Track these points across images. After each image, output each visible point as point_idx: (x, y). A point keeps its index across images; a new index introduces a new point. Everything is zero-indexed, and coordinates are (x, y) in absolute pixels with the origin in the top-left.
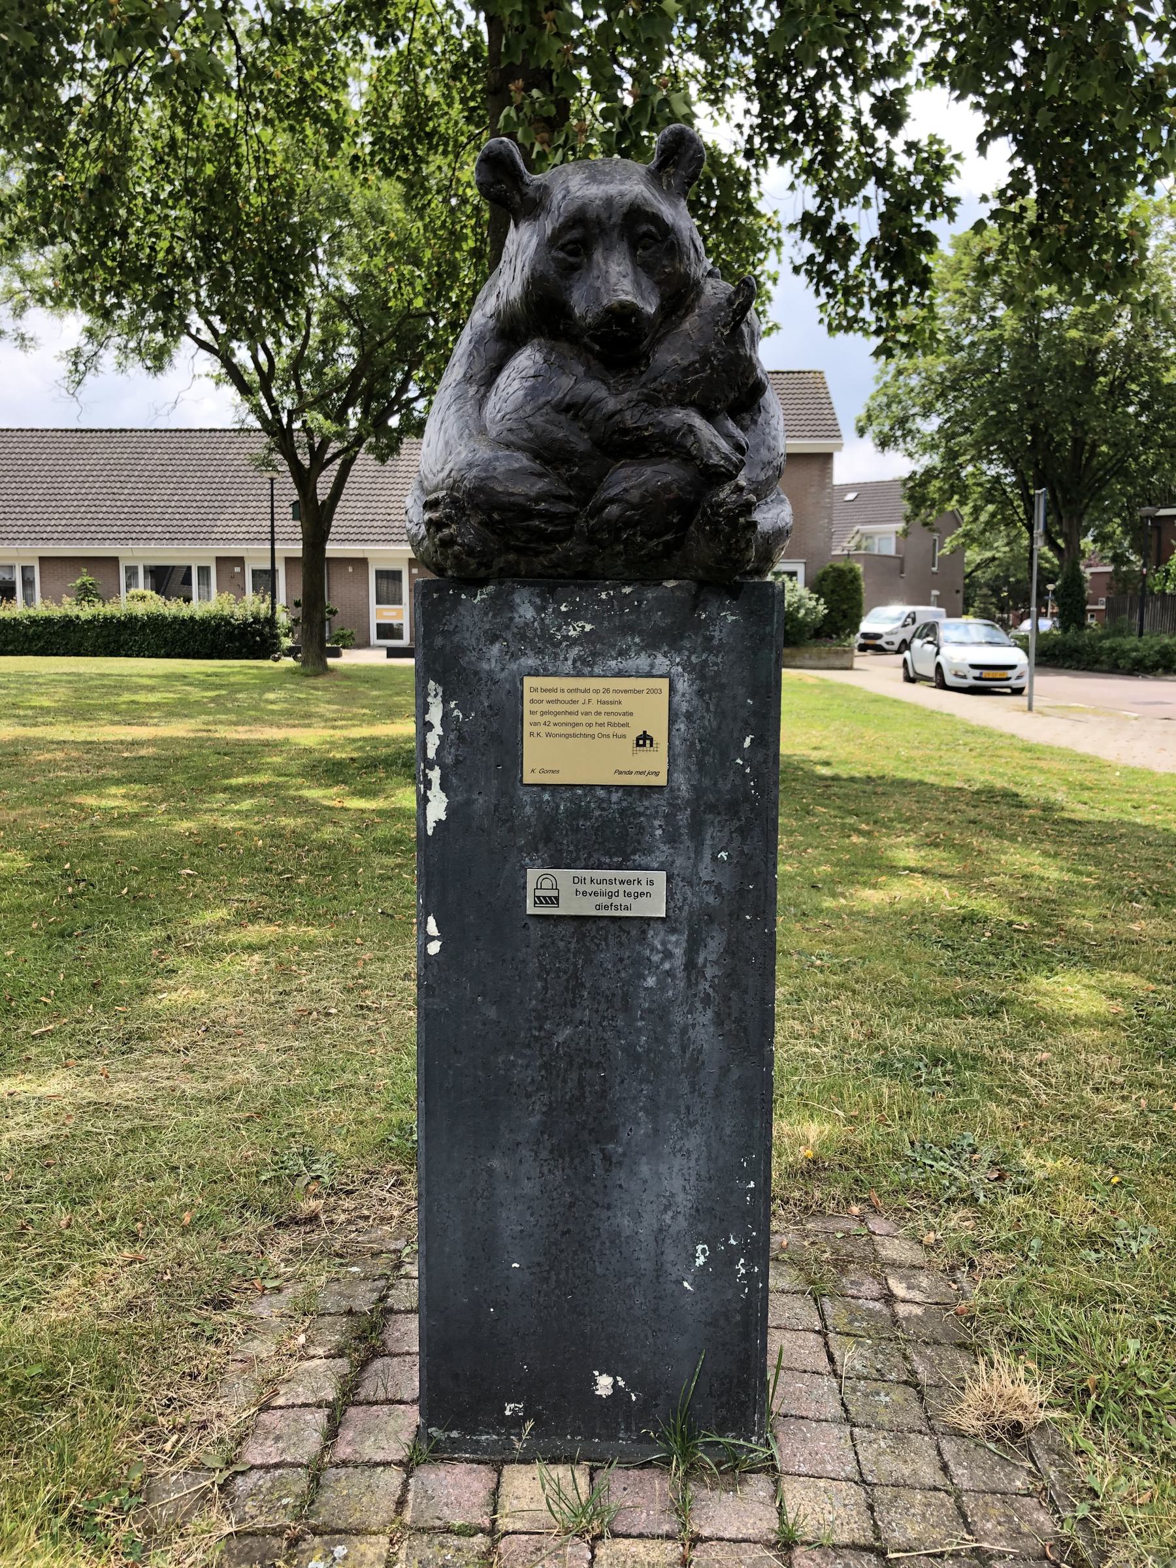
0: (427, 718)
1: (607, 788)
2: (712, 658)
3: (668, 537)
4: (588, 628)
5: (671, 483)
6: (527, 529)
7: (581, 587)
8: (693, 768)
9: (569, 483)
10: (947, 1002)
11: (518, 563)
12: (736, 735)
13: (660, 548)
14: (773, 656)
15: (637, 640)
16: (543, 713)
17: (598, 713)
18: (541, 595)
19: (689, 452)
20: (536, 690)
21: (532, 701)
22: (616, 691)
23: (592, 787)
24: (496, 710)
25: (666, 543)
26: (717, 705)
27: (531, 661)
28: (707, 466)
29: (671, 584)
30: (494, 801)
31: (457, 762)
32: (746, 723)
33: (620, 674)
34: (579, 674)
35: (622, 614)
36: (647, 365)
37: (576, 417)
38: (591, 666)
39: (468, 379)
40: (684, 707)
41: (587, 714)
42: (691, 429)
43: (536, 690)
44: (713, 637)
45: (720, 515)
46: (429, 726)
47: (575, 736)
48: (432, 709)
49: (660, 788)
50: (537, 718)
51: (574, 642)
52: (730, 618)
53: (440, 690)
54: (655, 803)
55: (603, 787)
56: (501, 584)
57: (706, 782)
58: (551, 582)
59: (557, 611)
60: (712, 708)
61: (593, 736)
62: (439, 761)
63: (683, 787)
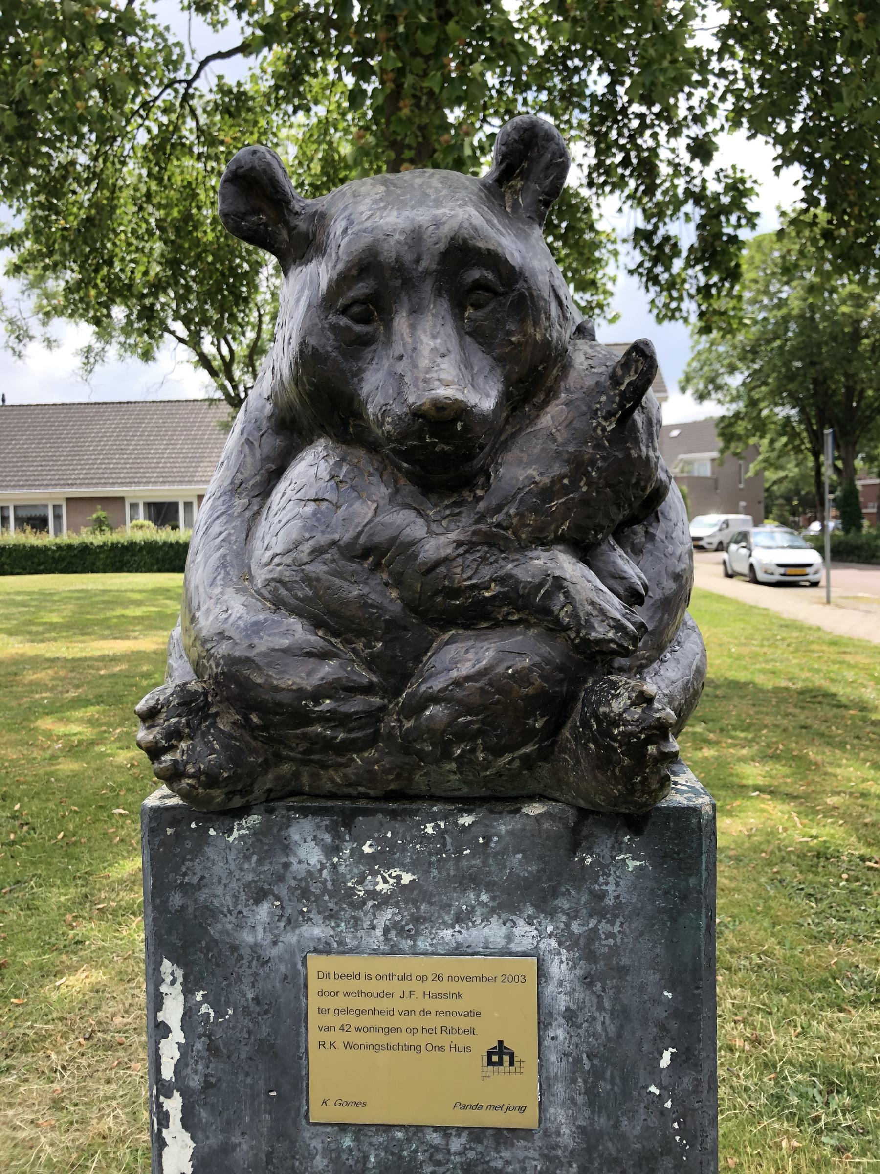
0: (161, 1016)
1: (444, 1131)
2: (604, 927)
3: (528, 749)
4: (407, 878)
5: (530, 670)
6: (305, 736)
7: (394, 815)
8: (580, 1099)
9: (371, 663)
10: (824, 984)
11: (296, 775)
12: (646, 1048)
13: (517, 763)
14: (703, 924)
15: (484, 898)
16: (338, 1012)
17: (425, 1013)
18: (332, 829)
19: (557, 621)
20: (327, 976)
21: (321, 993)
22: (452, 978)
23: (419, 1129)
24: (265, 1005)
25: (525, 758)
26: (616, 999)
27: (317, 930)
28: (586, 641)
29: (534, 809)
30: (265, 1147)
31: (208, 1086)
32: (663, 1028)
33: (458, 950)
34: (395, 950)
35: (460, 857)
36: (487, 485)
37: (376, 567)
38: (413, 938)
39: (235, 488)
40: (562, 1003)
41: (409, 1013)
42: (559, 583)
43: (327, 976)
44: (604, 894)
45: (614, 738)
46: (162, 1030)
47: (390, 1047)
48: (168, 1003)
49: (526, 1133)
50: (329, 1019)
51: (384, 901)
52: (632, 864)
53: (179, 974)
54: (521, 1154)
55: (436, 1129)
56: (270, 811)
57: (602, 1122)
58: (343, 810)
59: (358, 853)
60: (607, 1004)
61: (418, 1049)
62: (180, 1083)
63: (565, 1130)
